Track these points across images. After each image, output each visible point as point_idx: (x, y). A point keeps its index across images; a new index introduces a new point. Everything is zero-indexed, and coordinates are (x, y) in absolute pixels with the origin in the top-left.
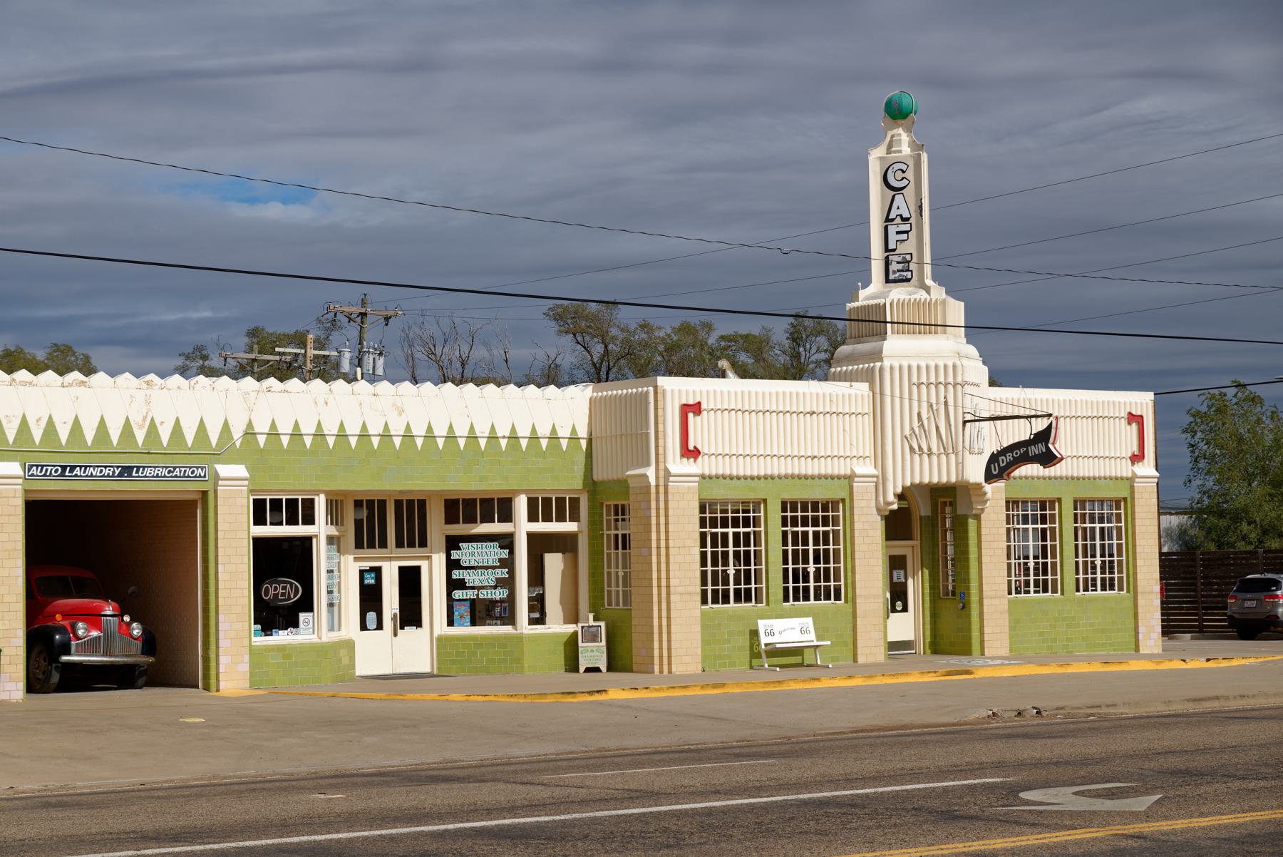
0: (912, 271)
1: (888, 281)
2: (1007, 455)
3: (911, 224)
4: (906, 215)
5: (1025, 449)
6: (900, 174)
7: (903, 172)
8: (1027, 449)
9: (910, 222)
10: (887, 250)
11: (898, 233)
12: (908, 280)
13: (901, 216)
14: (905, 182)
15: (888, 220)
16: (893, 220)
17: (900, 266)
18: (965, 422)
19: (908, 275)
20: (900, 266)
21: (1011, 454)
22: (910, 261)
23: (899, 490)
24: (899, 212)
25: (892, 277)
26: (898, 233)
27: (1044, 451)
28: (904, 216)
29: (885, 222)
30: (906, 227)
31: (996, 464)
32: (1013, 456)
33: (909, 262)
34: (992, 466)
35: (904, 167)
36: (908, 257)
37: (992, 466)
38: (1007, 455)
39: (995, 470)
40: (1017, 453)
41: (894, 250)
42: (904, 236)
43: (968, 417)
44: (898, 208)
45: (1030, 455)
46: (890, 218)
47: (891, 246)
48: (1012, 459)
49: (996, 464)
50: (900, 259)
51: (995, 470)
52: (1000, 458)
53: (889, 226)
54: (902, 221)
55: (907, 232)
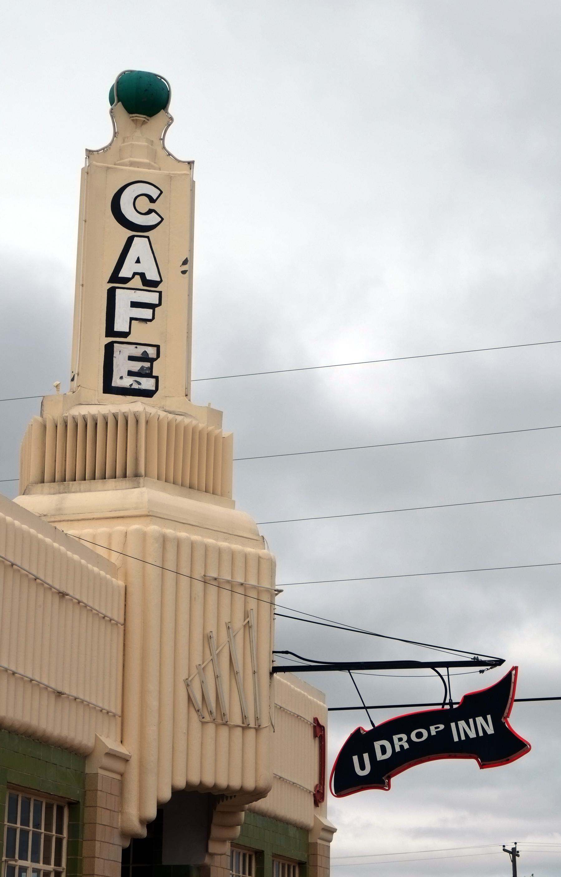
0: (157, 378)
1: (108, 388)
2: (395, 738)
3: (160, 293)
4: (152, 275)
5: (442, 727)
6: (144, 204)
7: (152, 200)
8: (448, 729)
9: (158, 289)
10: (110, 331)
11: (134, 305)
12: (148, 394)
13: (142, 275)
14: (152, 219)
15: (115, 278)
16: (126, 280)
17: (136, 366)
18: (276, 670)
19: (147, 384)
20: (136, 366)
21: (404, 737)
22: (155, 359)
23: (167, 795)
24: (139, 268)
25: (116, 382)
26: (134, 305)
27: (490, 730)
28: (148, 277)
29: (110, 281)
30: (152, 298)
31: (366, 756)
32: (409, 741)
33: (152, 361)
34: (355, 759)
35: (154, 193)
36: (152, 352)
37: (355, 759)
38: (395, 738)
39: (363, 767)
40: (419, 735)
41: (125, 335)
42: (147, 313)
43: (281, 661)
44: (138, 261)
45: (456, 739)
46: (120, 275)
47: (120, 325)
48: (406, 746)
49: (366, 756)
50: (138, 351)
51: (363, 767)
52: (377, 745)
53: (118, 291)
54: (144, 285)
55: (152, 306)
